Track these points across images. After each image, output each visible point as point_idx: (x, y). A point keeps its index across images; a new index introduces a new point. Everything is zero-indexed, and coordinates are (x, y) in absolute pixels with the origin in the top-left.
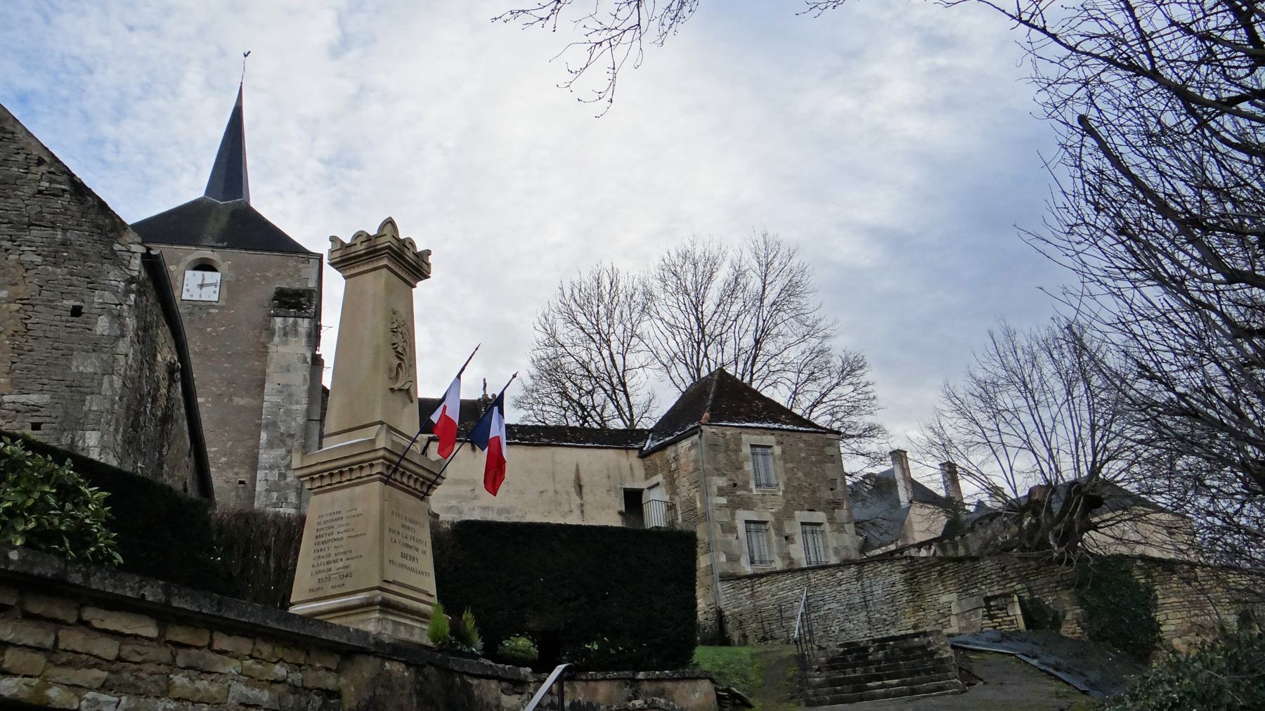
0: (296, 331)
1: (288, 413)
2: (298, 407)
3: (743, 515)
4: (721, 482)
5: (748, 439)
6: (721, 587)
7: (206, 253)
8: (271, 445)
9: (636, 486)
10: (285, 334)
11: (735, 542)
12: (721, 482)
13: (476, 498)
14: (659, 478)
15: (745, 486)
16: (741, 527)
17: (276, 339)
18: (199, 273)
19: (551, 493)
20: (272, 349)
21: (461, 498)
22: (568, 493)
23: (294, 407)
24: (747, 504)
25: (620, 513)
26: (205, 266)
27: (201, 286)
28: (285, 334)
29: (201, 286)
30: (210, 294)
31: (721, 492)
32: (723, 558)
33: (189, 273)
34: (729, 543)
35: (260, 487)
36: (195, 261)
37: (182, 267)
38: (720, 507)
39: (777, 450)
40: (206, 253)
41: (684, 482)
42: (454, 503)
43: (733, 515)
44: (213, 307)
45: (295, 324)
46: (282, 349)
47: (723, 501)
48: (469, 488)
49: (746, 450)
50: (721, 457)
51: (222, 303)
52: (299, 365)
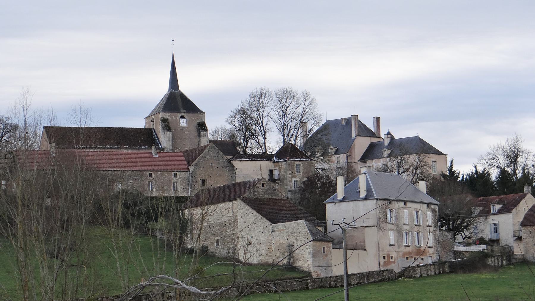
3: (294, 179)
4: (290, 172)
5: (296, 163)
7: (183, 114)
12: (290, 172)
14: (277, 168)
15: (295, 173)
24: (294, 177)
26: (182, 117)
30: (185, 124)
31: (290, 174)
39: (302, 165)
40: (183, 114)
41: (282, 171)
49: (295, 165)
50: (291, 167)
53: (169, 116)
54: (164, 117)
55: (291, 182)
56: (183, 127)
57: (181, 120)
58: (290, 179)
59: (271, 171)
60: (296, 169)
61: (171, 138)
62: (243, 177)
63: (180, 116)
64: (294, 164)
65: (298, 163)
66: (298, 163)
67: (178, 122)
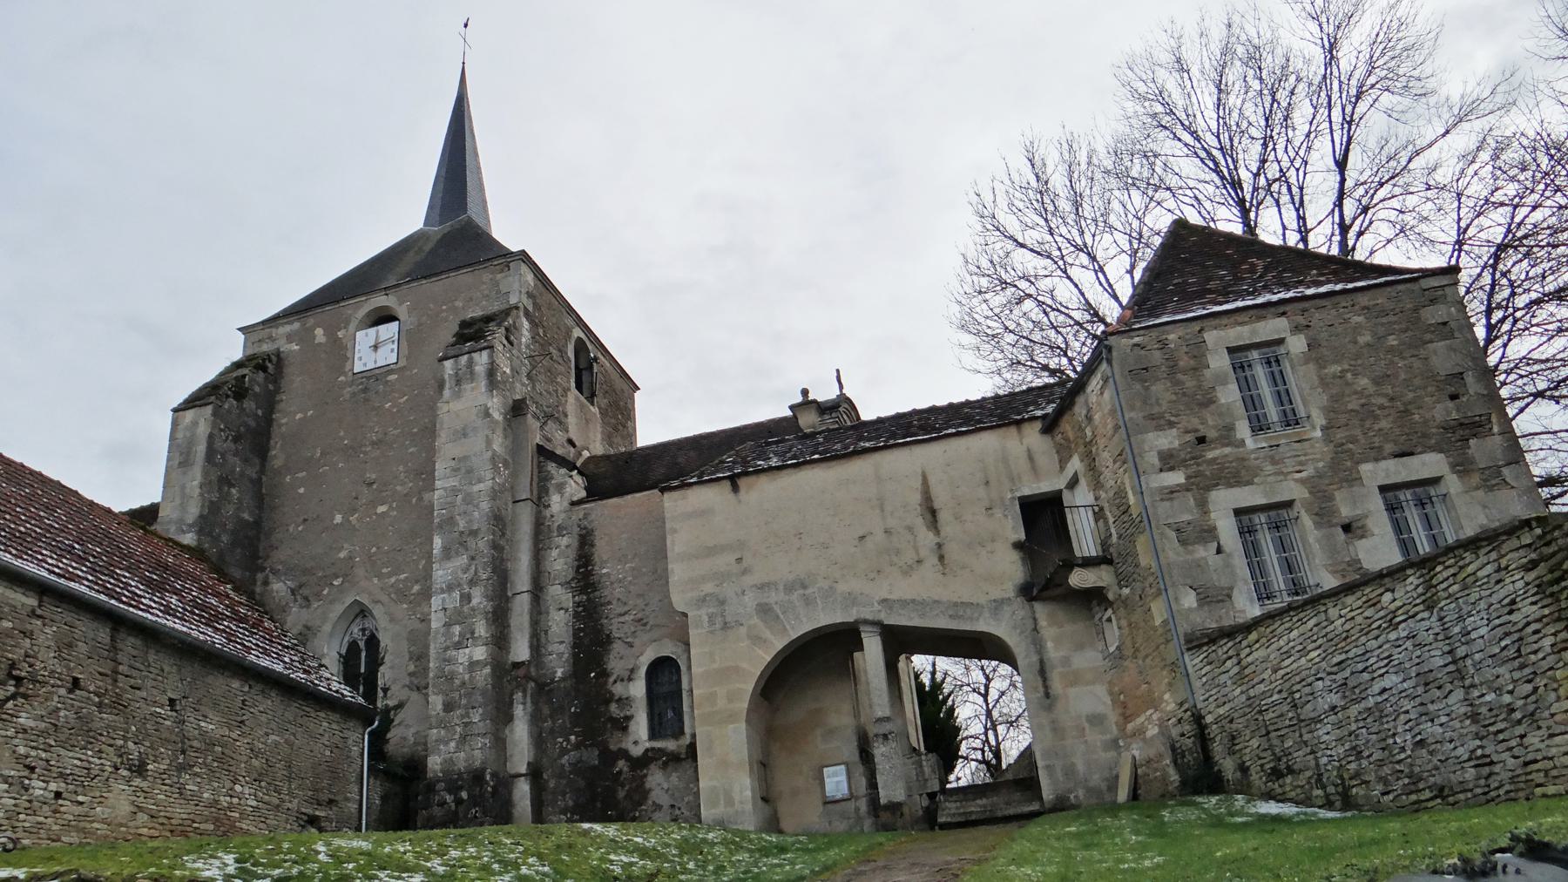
0: (472, 373)
1: (469, 500)
2: (481, 486)
3: (1225, 501)
5: (1218, 339)
6: (1193, 661)
7: (380, 300)
8: (447, 553)
9: (1045, 486)
10: (458, 382)
11: (1213, 560)
12: (1167, 440)
13: (745, 572)
14: (1075, 464)
15: (1227, 435)
16: (1227, 528)
17: (447, 393)
18: (372, 331)
19: (879, 536)
20: (443, 408)
21: (721, 577)
22: (910, 529)
23: (476, 488)
24: (1235, 476)
25: (1018, 546)
27: (376, 347)
28: (458, 382)
29: (376, 347)
30: (388, 356)
31: (1168, 461)
32: (1189, 600)
33: (359, 334)
34: (1200, 565)
35: (436, 623)
36: (368, 314)
37: (352, 327)
38: (1171, 493)
39: (1297, 344)
40: (380, 300)
42: (709, 588)
43: (1203, 505)
44: (391, 372)
45: (471, 363)
46: (456, 406)
47: (1177, 478)
48: (731, 558)
49: (1219, 362)
50: (1161, 391)
51: (401, 364)
52: (479, 422)
53: (290, 338)
54: (266, 347)
55: (1208, 533)
56: (376, 376)
57: (365, 338)
58: (1184, 511)
59: (1043, 517)
60: (1230, 395)
61: (201, 449)
62: (764, 610)
63: (362, 313)
64: (1198, 351)
65: (1240, 334)
66: (1240, 334)
67: (341, 352)
